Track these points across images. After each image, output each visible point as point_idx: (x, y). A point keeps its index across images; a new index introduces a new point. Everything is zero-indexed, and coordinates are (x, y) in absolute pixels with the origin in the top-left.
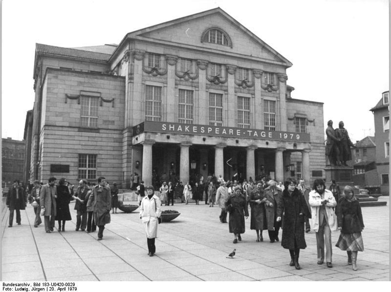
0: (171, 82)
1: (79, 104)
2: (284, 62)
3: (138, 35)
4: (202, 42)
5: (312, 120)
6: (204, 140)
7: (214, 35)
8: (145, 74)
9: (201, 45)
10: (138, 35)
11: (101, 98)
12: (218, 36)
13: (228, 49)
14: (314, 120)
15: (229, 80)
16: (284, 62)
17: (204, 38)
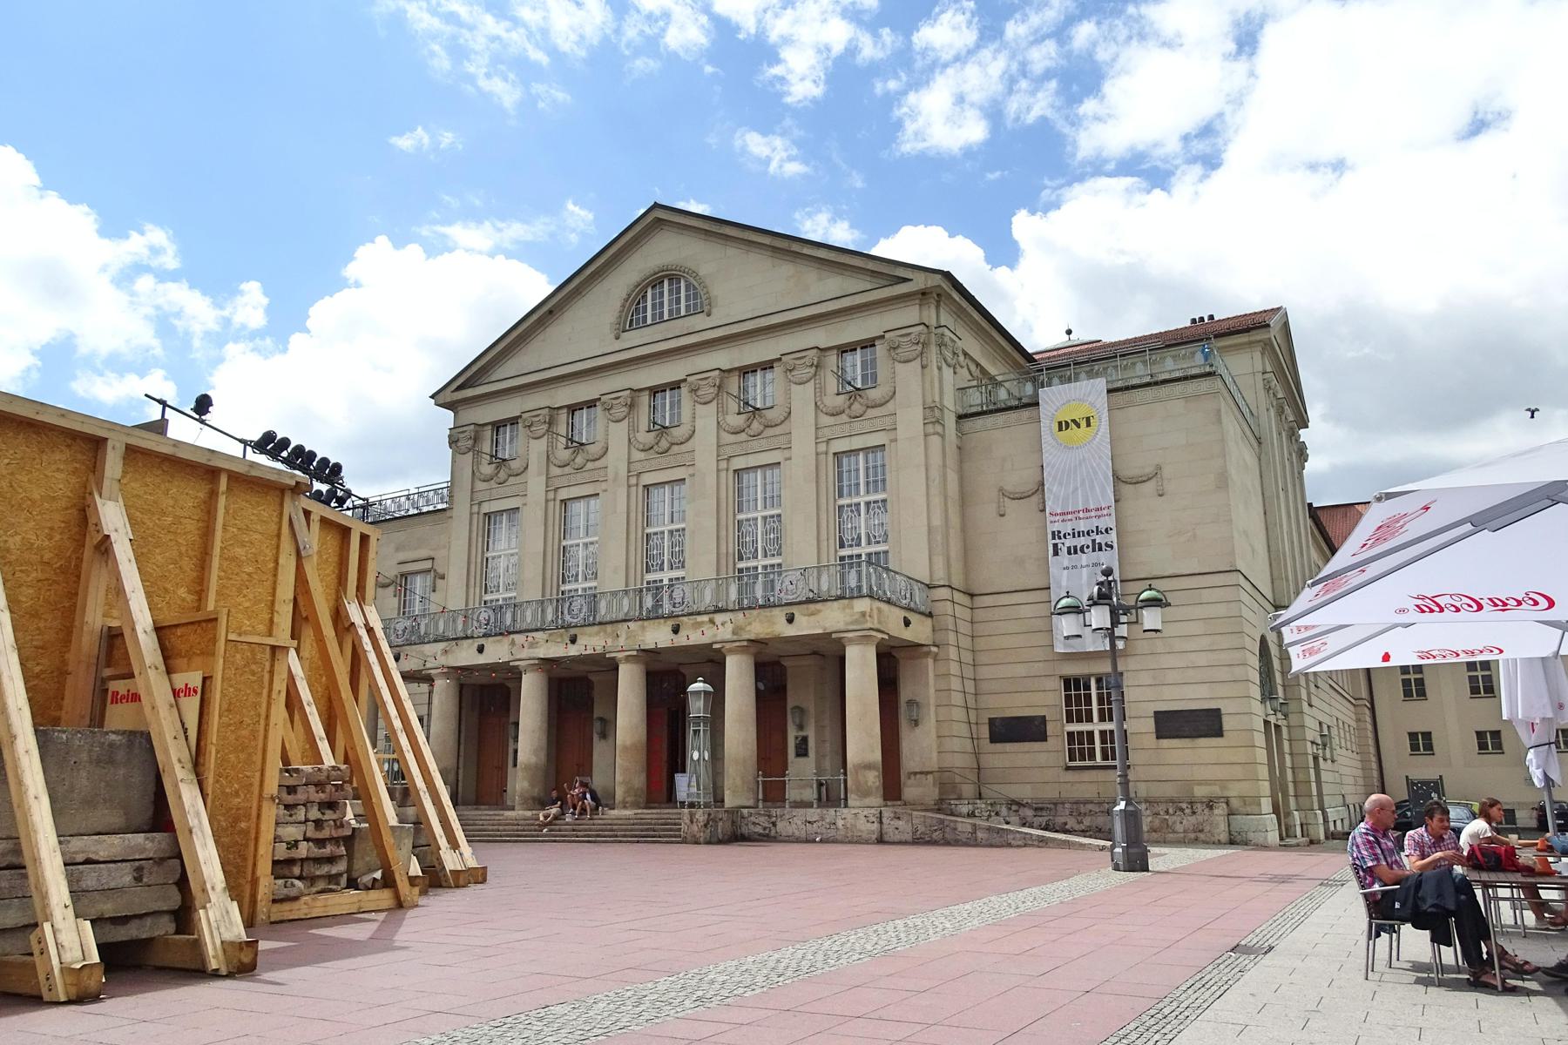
0: (535, 484)
1: (395, 596)
2: (905, 280)
3: (459, 388)
4: (617, 338)
5: (1149, 470)
6: (481, 649)
7: (662, 294)
8: (480, 486)
9: (618, 345)
10: (459, 388)
11: (435, 571)
12: (670, 291)
13: (699, 322)
14: (1159, 467)
15: (699, 424)
16: (905, 280)
17: (632, 315)
